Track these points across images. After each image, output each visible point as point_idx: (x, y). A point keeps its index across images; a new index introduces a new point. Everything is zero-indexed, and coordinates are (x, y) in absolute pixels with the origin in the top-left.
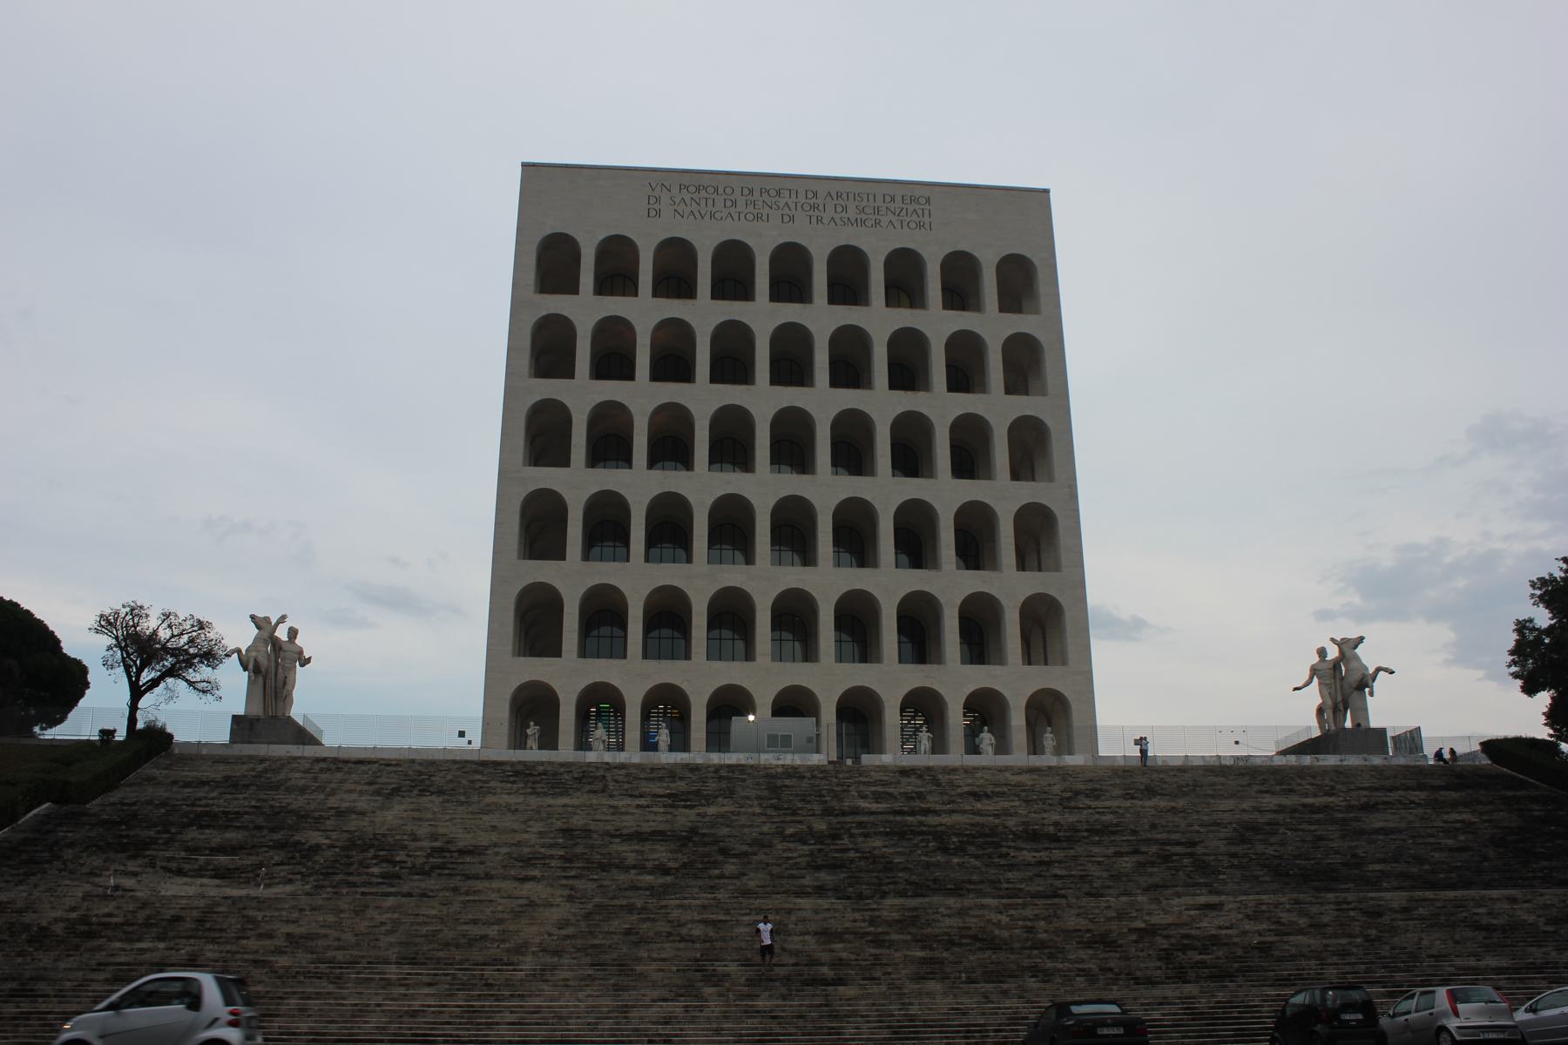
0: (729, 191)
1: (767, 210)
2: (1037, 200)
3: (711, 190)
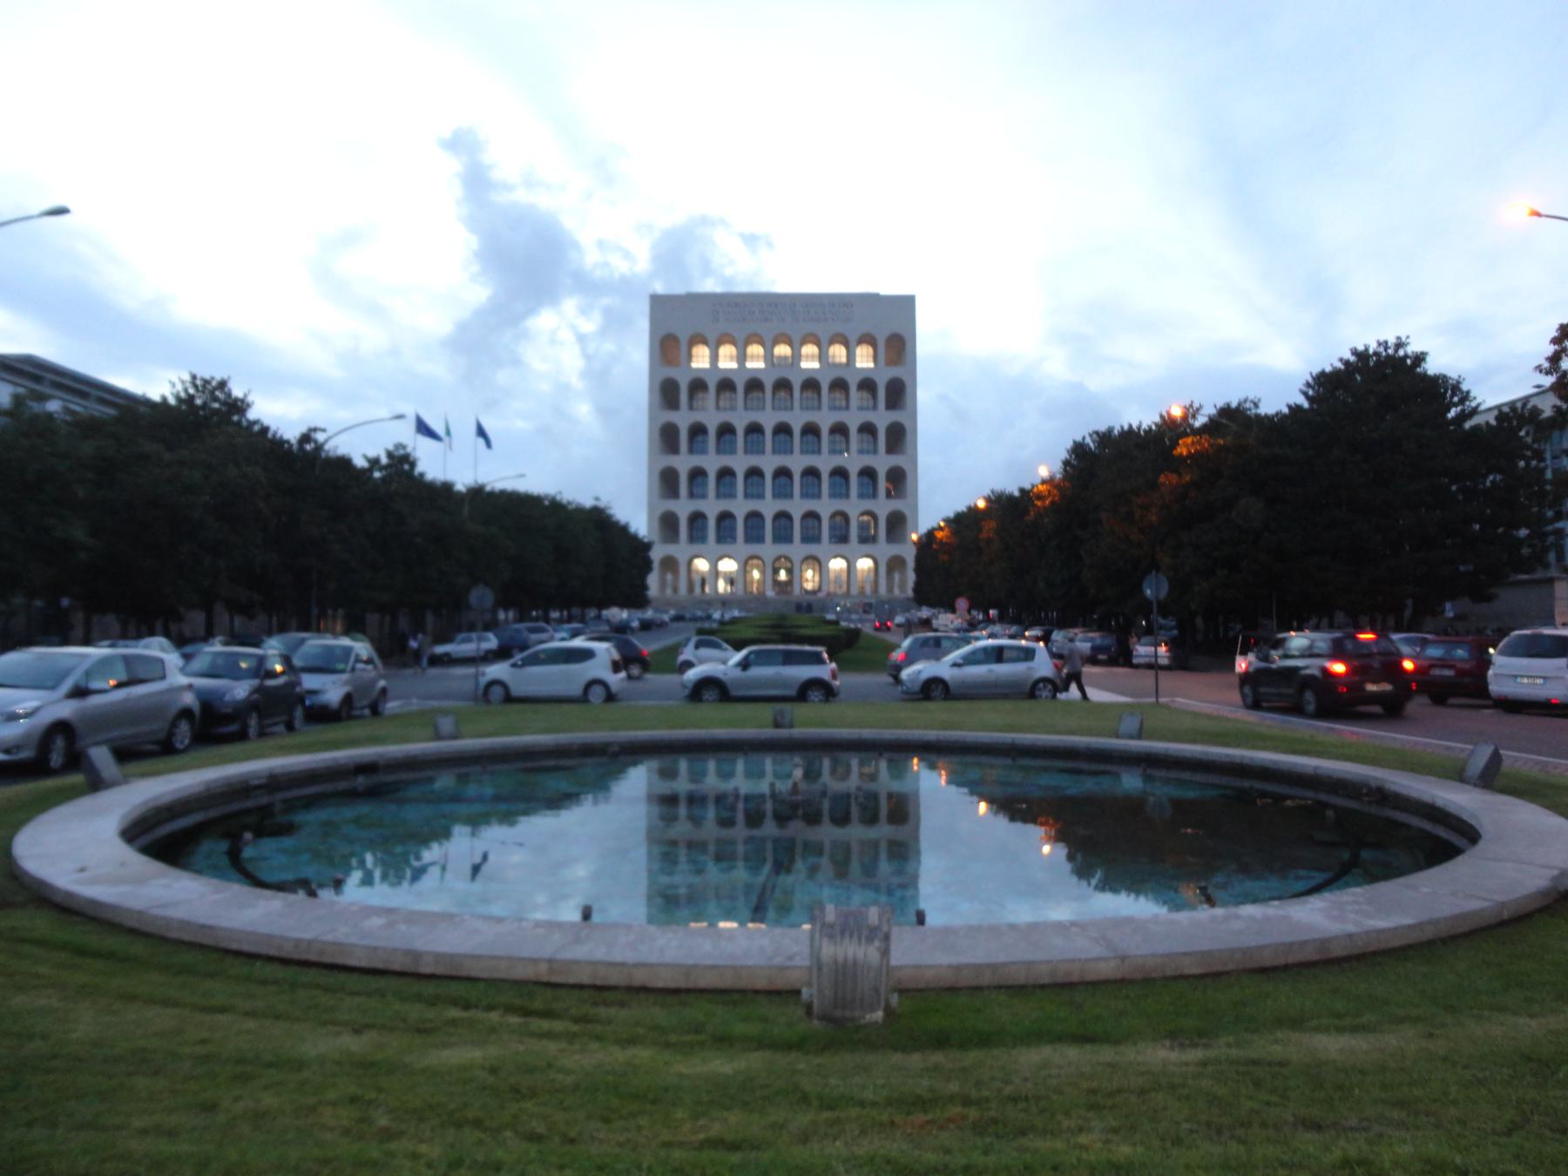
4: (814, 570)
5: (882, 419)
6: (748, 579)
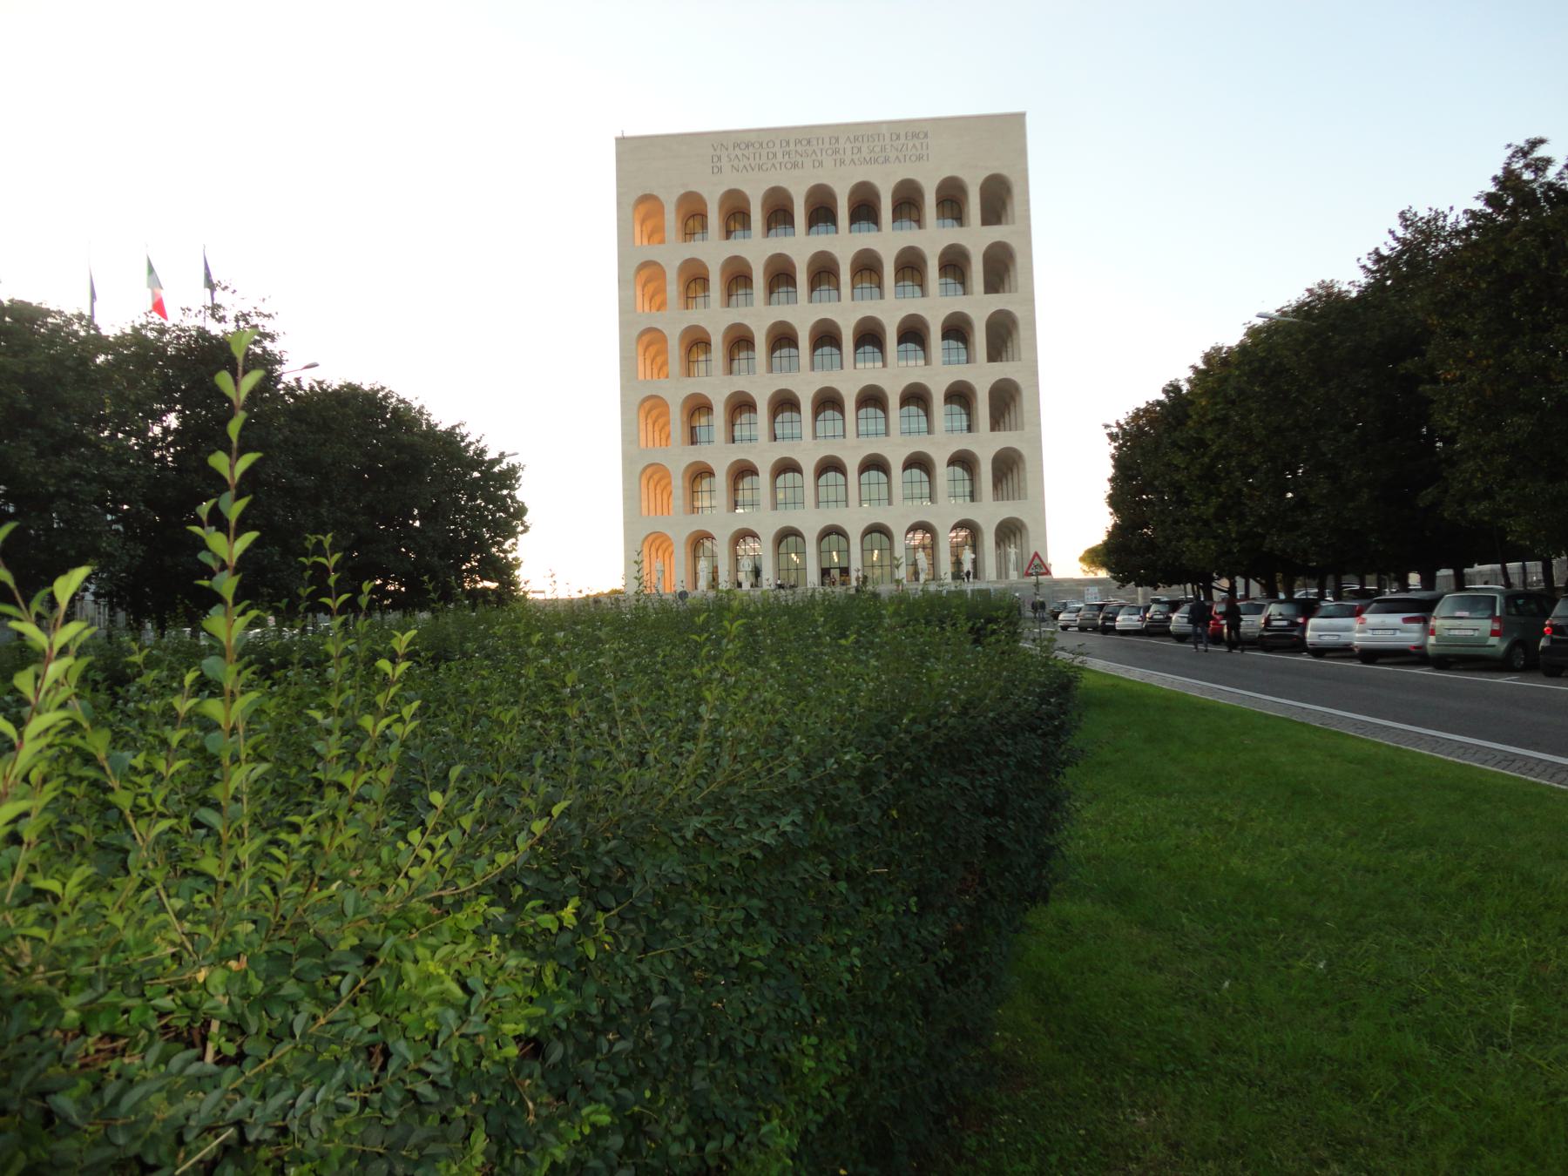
0: (771, 145)
1: (799, 159)
3: (757, 145)
4: (881, 550)
5: (979, 306)
6: (783, 565)
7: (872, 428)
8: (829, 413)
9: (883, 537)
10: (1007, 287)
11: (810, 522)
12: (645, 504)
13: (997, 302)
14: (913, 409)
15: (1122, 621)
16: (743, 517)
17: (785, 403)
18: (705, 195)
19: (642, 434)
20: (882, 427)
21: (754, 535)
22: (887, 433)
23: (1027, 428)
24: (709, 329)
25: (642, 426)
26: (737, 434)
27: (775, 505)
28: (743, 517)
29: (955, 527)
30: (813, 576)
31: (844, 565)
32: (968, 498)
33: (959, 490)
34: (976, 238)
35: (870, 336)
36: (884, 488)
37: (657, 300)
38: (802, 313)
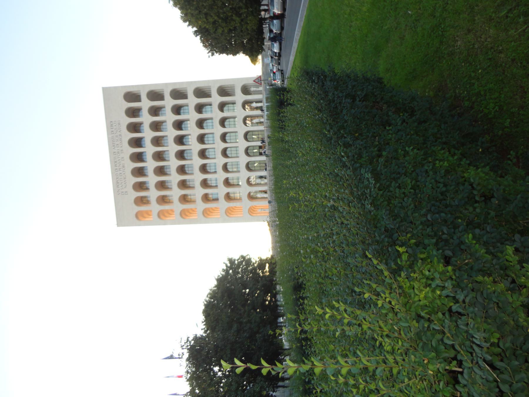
0: (117, 175)
1: (121, 165)
2: (107, 91)
3: (117, 180)
4: (253, 135)
6: (259, 168)
7: (211, 139)
8: (207, 154)
9: (248, 134)
10: (162, 93)
11: (244, 159)
12: (239, 215)
13: (167, 96)
14: (205, 125)
15: (276, 50)
16: (242, 182)
17: (204, 169)
18: (135, 197)
19: (216, 217)
20: (211, 135)
21: (249, 178)
22: (213, 133)
23: (210, 85)
24: (180, 195)
25: (213, 217)
26: (214, 185)
27: (239, 172)
28: (242, 182)
29: (245, 109)
30: (263, 158)
31: (258, 148)
32: (235, 105)
33: (232, 108)
34: (145, 104)
35: (180, 140)
36: (232, 134)
37: (170, 212)
38: (173, 163)
